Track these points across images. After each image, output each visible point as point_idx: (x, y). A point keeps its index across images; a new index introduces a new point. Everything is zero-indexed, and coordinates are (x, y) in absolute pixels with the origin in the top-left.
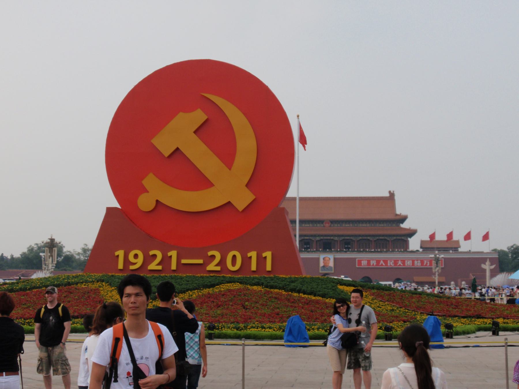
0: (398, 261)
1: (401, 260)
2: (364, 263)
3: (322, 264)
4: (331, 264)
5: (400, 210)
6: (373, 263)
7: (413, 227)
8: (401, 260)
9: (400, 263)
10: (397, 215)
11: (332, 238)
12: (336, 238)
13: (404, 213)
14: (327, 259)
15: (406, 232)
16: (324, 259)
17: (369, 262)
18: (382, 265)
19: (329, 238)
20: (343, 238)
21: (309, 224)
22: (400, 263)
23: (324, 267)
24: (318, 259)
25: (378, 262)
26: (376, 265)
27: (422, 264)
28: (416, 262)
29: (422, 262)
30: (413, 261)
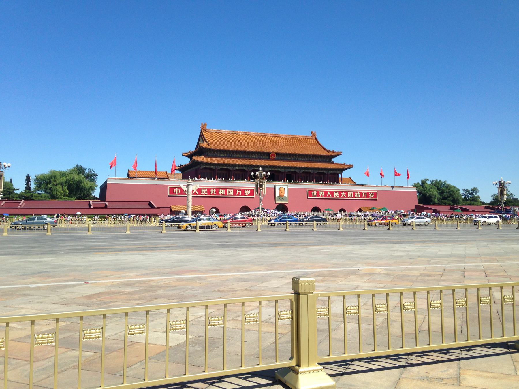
0: (342, 192)
1: (345, 192)
2: (314, 194)
3: (277, 194)
4: (286, 194)
5: (331, 146)
6: (322, 193)
7: (348, 163)
8: (345, 192)
9: (343, 194)
10: (329, 151)
11: (279, 170)
12: (283, 170)
13: (337, 150)
14: (282, 189)
15: (341, 167)
16: (279, 189)
17: (318, 192)
18: (329, 196)
19: (277, 169)
20: (289, 170)
21: (255, 155)
22: (343, 194)
23: (279, 196)
24: (275, 188)
25: (326, 193)
26: (324, 196)
27: (361, 196)
28: (356, 194)
29: (361, 193)
30: (354, 193)
